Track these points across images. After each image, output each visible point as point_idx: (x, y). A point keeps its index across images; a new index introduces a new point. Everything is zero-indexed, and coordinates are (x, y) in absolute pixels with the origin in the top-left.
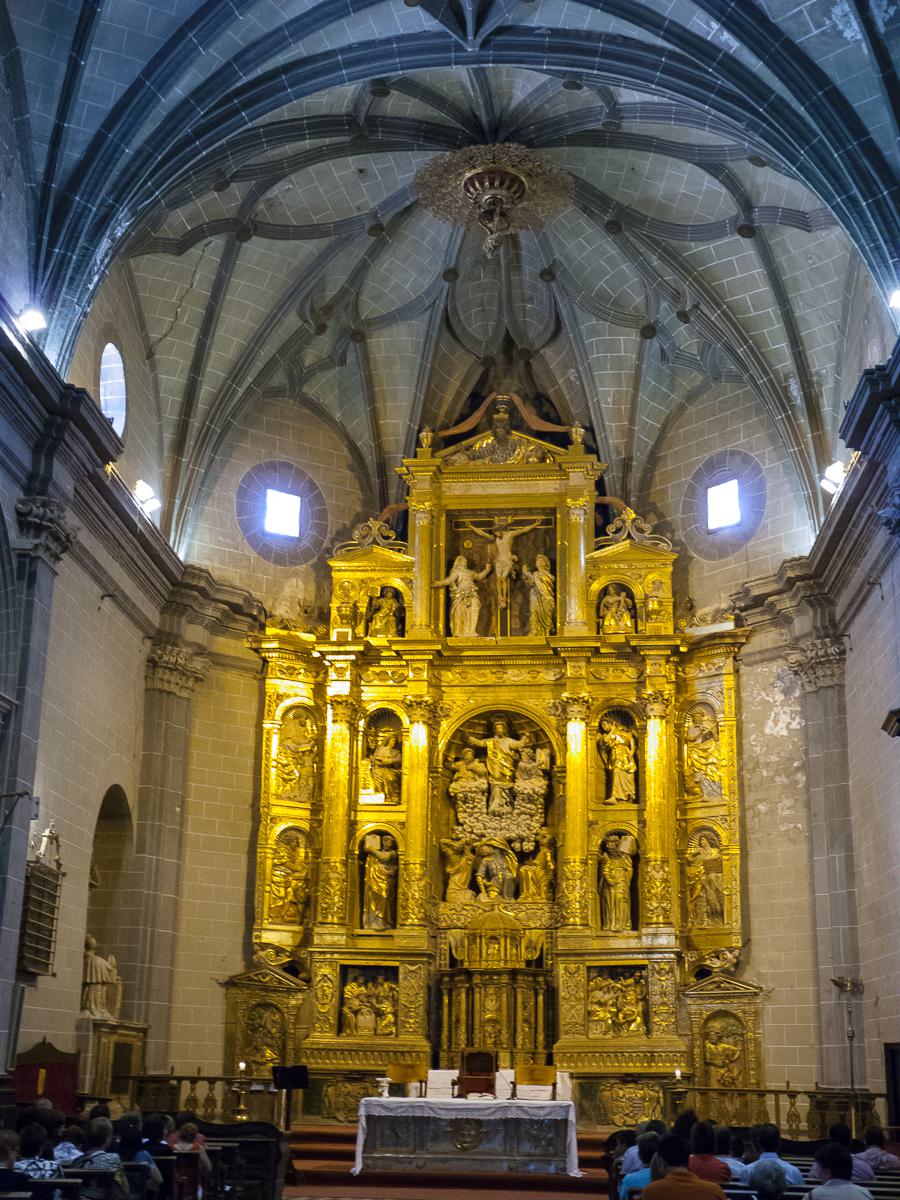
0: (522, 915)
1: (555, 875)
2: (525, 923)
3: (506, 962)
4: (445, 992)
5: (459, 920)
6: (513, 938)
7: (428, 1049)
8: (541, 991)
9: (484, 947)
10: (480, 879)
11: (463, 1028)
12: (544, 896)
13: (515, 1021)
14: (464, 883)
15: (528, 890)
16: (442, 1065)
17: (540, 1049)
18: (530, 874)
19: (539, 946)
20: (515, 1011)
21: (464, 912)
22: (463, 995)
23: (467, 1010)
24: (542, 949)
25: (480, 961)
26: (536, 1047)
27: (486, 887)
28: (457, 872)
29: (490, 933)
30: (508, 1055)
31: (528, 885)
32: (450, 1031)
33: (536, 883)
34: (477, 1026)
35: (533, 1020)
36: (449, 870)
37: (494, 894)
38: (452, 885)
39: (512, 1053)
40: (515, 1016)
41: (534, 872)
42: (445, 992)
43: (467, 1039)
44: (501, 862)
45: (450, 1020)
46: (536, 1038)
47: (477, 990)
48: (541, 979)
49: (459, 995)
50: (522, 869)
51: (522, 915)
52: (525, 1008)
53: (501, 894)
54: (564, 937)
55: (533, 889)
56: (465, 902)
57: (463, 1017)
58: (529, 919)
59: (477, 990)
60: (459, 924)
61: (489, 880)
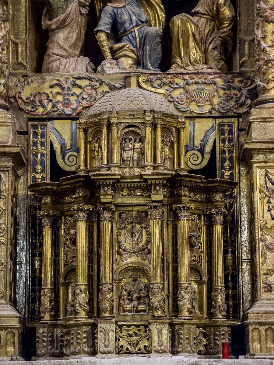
0: (176, 94)
1: (234, 29)
2: (183, 107)
3: (154, 168)
4: (46, 222)
5: (67, 103)
6: (166, 130)
7: (15, 322)
8: (219, 219)
9: (116, 147)
10: (102, 37)
11: (82, 282)
12: (212, 64)
13: (176, 269)
14: (74, 46)
15: (188, 53)
16: (41, 350)
17: (220, 318)
18: (191, 28)
19: (208, 149)
20: (176, 252)
21: (77, 91)
22: (82, 225)
23: (90, 252)
24: (213, 151)
25: (109, 168)
26: (211, 315)
27: (113, 52)
28: (62, 25)
29: (128, 120)
30: (166, 331)
31: (186, 47)
32: (55, 290)
33: (201, 43)
34: (106, 279)
35: (204, 268)
36: (45, 23)
37: (127, 63)
38: (54, 49)
39: (172, 325)
40: (176, 260)
41: (197, 26)
42: (46, 222)
43: (90, 302)
44: (137, 10)
45: (56, 271)
46: (211, 300)
47: (106, 215)
48: (218, 197)
49: (74, 226)
50: (178, 20)
51: (176, 94)
52: (192, 246)
53: (138, 63)
54: (265, 120)
55: (195, 53)
56: (77, 74)
57: (82, 263)
58: (191, 99)
59: (106, 215)
60: (68, 111)
61: (118, 41)
